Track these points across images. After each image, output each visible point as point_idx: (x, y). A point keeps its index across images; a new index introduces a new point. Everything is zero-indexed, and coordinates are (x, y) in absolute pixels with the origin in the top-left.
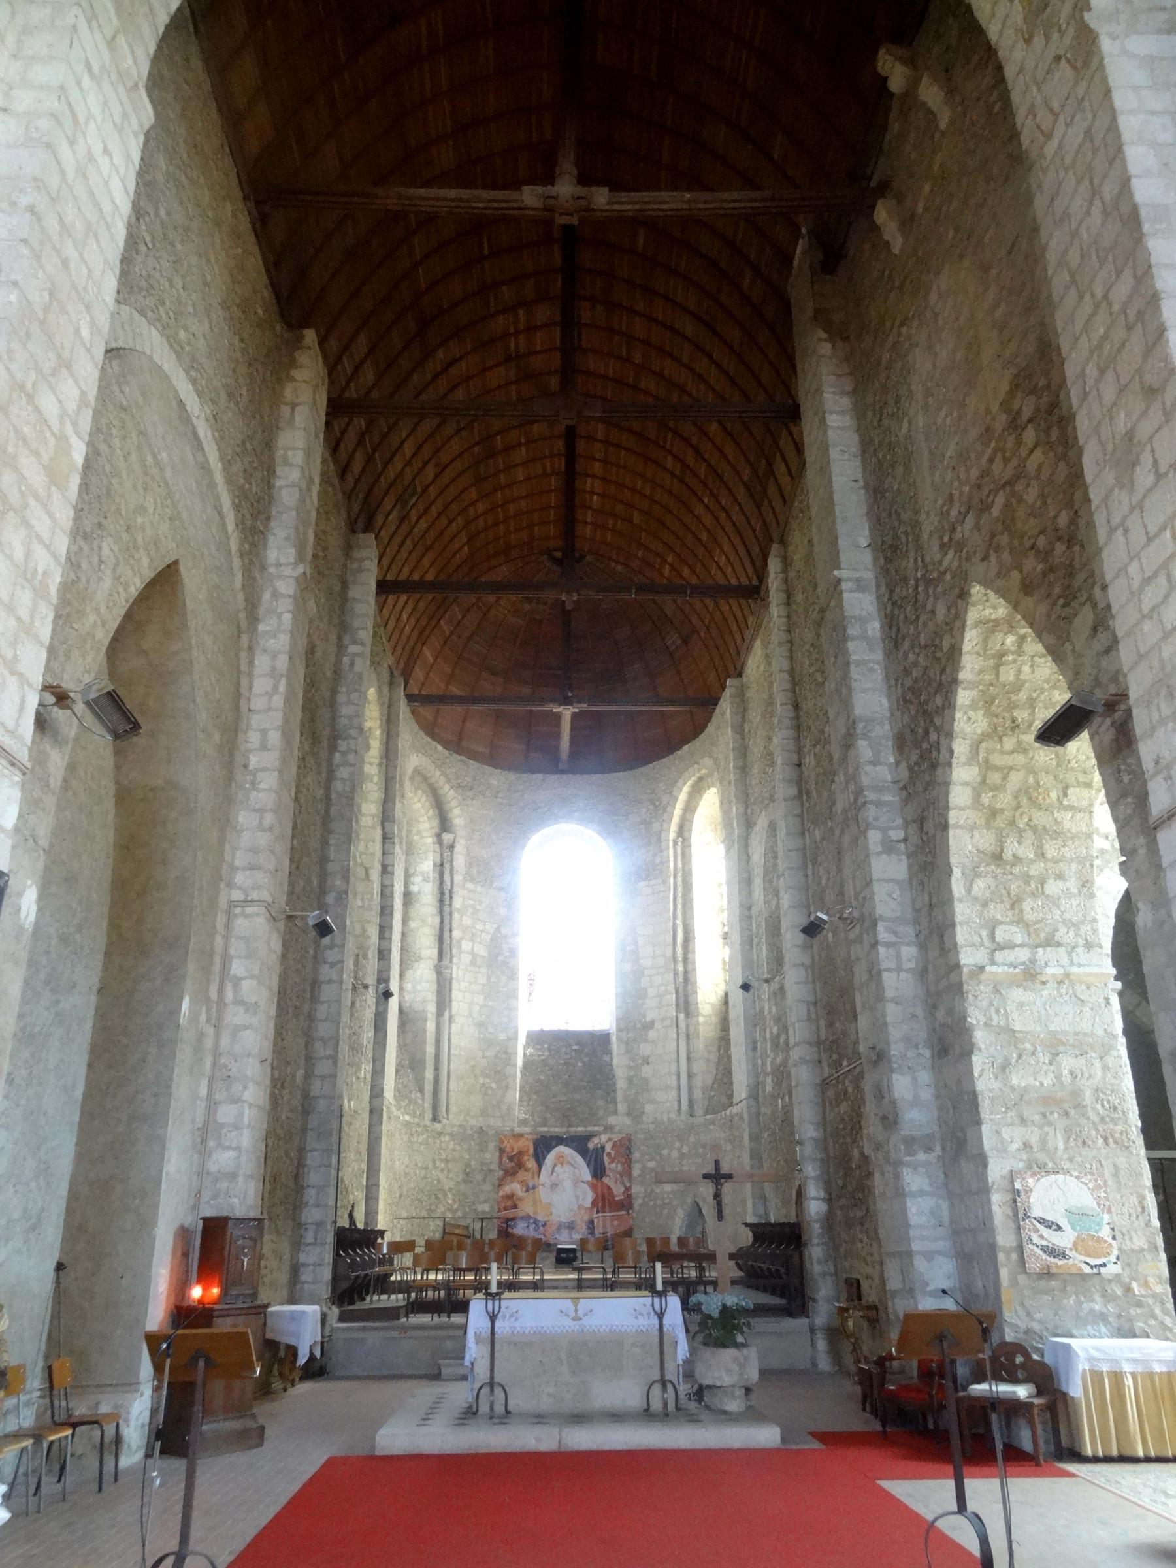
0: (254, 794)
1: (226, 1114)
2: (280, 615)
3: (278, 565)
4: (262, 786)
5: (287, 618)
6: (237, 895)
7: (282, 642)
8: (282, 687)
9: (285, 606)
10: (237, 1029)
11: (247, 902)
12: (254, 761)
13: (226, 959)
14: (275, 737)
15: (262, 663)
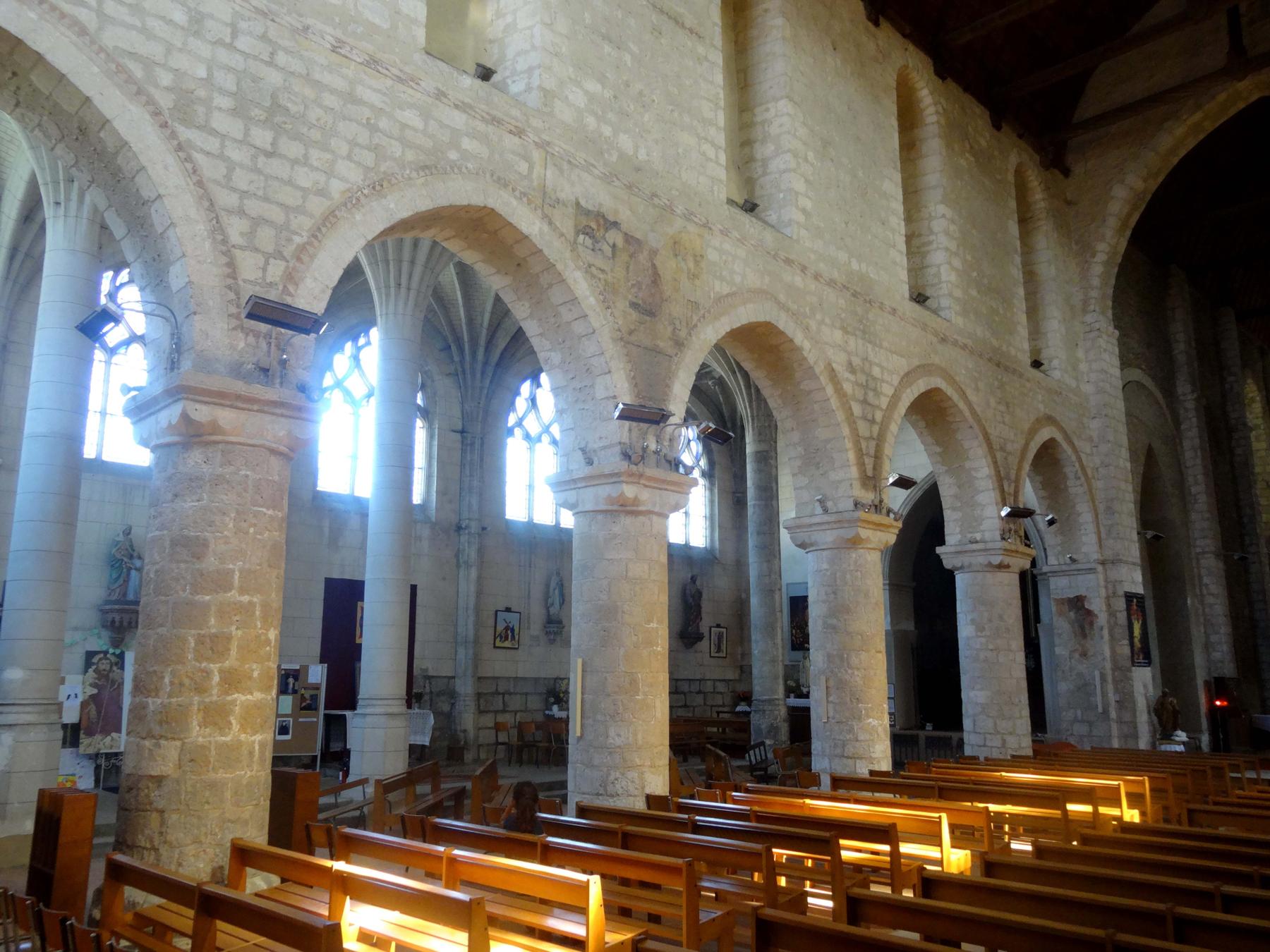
0: (1196, 505)
1: (1214, 638)
2: (1190, 419)
3: (1184, 395)
4: (1200, 501)
5: (1194, 420)
6: (1198, 550)
7: (1194, 432)
8: (1199, 454)
9: (1192, 414)
10: (1211, 606)
11: (1204, 553)
12: (1193, 490)
13: (1200, 577)
14: (1200, 478)
15: (1187, 444)
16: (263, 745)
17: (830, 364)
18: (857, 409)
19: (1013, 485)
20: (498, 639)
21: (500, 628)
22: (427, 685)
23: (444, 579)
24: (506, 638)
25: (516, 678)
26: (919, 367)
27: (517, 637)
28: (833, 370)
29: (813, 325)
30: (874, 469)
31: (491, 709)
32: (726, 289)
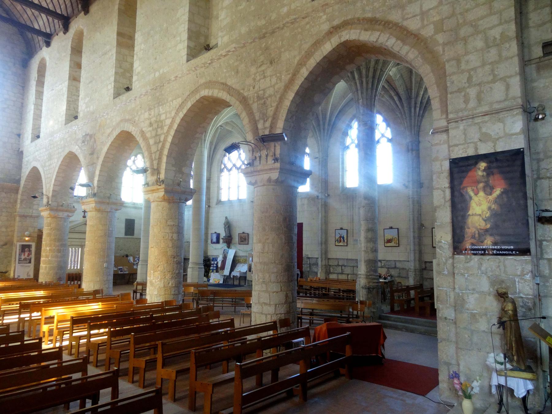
16: (46, 267)
17: (142, 130)
18: (151, 142)
19: (270, 120)
20: (337, 242)
21: (337, 237)
22: (308, 261)
23: (313, 219)
24: (340, 241)
25: (347, 259)
26: (189, 95)
27: (346, 241)
28: (143, 131)
29: (137, 119)
30: (158, 164)
31: (336, 272)
32: (111, 129)
